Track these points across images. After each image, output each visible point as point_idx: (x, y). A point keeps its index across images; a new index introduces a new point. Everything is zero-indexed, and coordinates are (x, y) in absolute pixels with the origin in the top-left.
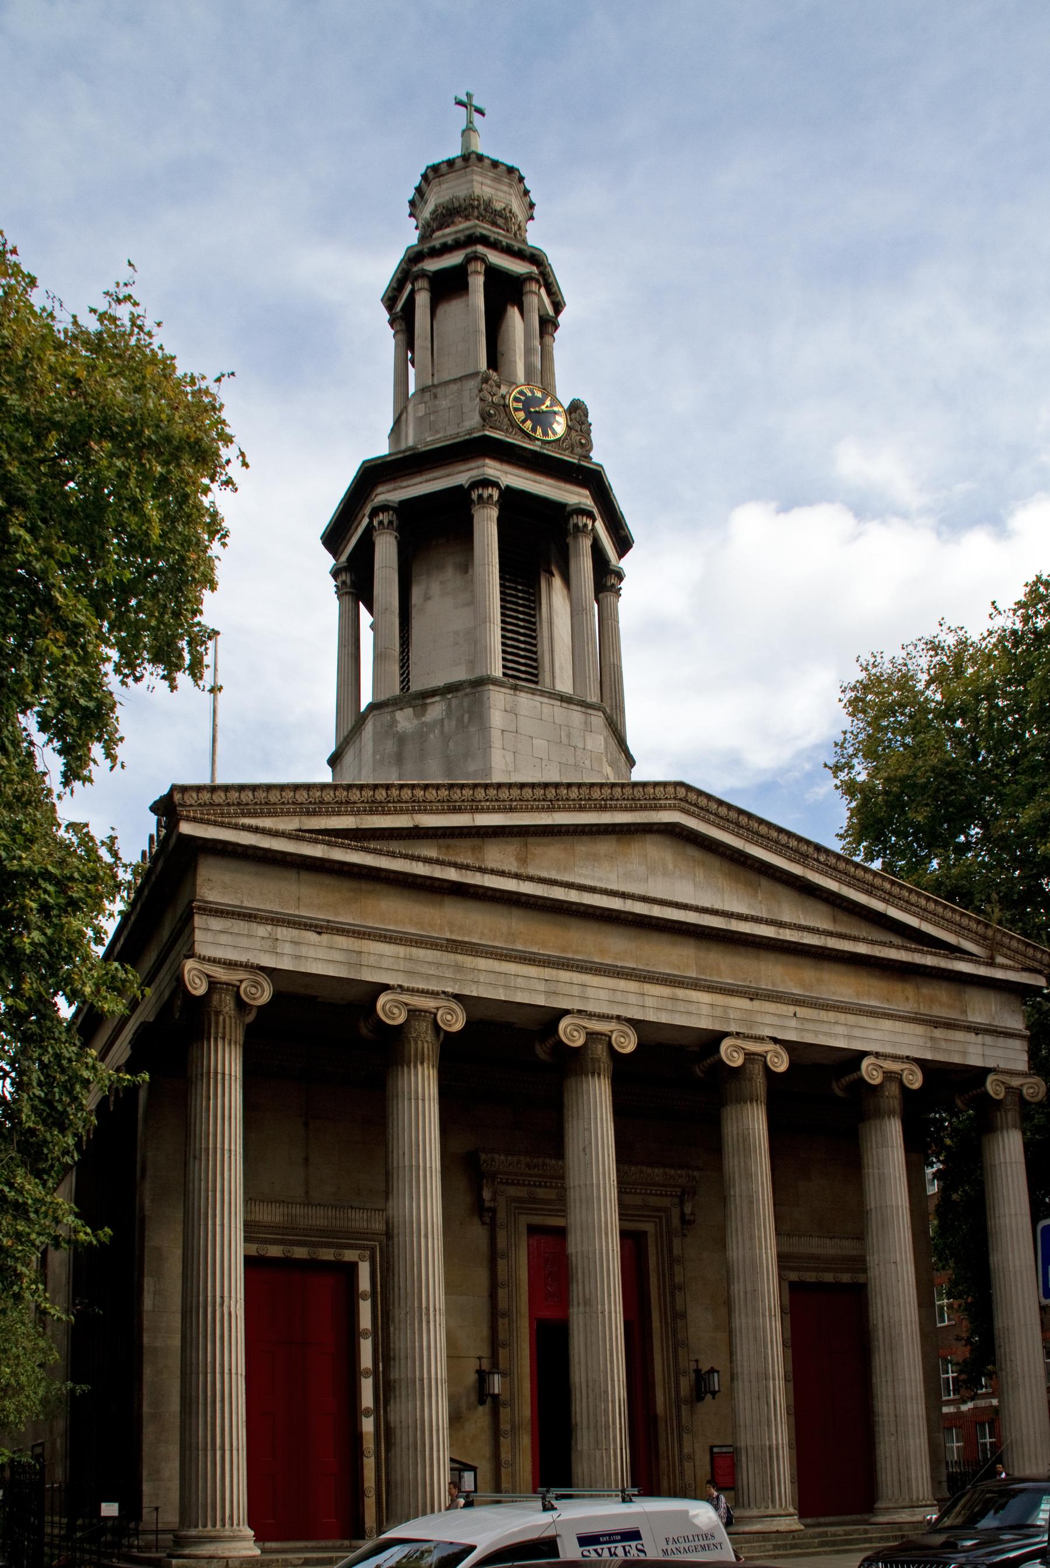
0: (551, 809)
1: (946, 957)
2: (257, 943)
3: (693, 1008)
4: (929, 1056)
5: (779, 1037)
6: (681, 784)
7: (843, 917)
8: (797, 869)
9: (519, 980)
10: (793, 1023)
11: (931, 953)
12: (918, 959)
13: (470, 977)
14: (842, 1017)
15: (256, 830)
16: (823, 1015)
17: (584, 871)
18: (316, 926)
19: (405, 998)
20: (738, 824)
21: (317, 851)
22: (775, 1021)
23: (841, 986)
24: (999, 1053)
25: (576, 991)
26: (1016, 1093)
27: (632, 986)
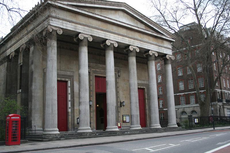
0: (106, 5)
1: (161, 35)
2: (60, 23)
7: (147, 27)
8: (141, 19)
9: (100, 33)
10: (140, 44)
15: (59, 3)
16: (144, 43)
18: (69, 21)
19: (83, 35)
23: (146, 38)
24: (168, 51)
25: (109, 36)
26: (170, 58)
27: (117, 36)
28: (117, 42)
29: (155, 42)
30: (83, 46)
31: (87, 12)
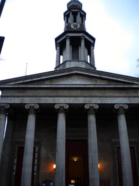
1: (131, 85)
3: (79, 100)
4: (129, 103)
6: (76, 67)
10: (99, 100)
11: (127, 85)
12: (124, 86)
14: (110, 98)
15: (8, 85)
16: (106, 98)
17: (61, 83)
20: (87, 71)
21: (17, 86)
22: (96, 100)
25: (58, 100)
27: (68, 98)
28: (68, 104)
29: (124, 93)
30: (119, 114)
31: (37, 85)
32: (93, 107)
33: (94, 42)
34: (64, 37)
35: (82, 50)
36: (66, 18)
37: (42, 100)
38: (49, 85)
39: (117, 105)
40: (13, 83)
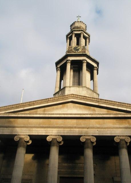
5: (94, 135)
9: (40, 131)
13: (31, 132)
17: (55, 111)
25: (51, 132)
28: (61, 136)
29: (126, 124)
32: (90, 139)
33: (98, 66)
34: (65, 61)
35: (86, 75)
36: (68, 40)
37: (33, 131)
38: (42, 114)
39: (117, 137)
40: (3, 112)
